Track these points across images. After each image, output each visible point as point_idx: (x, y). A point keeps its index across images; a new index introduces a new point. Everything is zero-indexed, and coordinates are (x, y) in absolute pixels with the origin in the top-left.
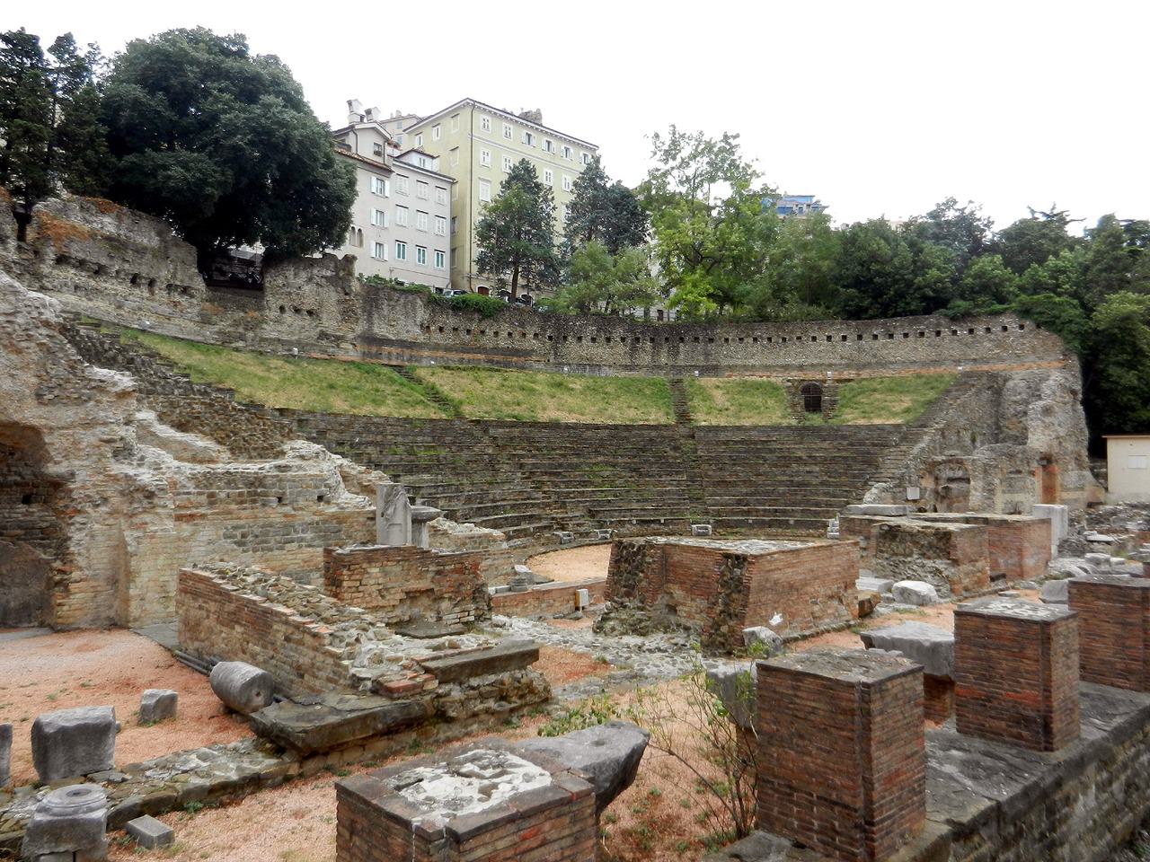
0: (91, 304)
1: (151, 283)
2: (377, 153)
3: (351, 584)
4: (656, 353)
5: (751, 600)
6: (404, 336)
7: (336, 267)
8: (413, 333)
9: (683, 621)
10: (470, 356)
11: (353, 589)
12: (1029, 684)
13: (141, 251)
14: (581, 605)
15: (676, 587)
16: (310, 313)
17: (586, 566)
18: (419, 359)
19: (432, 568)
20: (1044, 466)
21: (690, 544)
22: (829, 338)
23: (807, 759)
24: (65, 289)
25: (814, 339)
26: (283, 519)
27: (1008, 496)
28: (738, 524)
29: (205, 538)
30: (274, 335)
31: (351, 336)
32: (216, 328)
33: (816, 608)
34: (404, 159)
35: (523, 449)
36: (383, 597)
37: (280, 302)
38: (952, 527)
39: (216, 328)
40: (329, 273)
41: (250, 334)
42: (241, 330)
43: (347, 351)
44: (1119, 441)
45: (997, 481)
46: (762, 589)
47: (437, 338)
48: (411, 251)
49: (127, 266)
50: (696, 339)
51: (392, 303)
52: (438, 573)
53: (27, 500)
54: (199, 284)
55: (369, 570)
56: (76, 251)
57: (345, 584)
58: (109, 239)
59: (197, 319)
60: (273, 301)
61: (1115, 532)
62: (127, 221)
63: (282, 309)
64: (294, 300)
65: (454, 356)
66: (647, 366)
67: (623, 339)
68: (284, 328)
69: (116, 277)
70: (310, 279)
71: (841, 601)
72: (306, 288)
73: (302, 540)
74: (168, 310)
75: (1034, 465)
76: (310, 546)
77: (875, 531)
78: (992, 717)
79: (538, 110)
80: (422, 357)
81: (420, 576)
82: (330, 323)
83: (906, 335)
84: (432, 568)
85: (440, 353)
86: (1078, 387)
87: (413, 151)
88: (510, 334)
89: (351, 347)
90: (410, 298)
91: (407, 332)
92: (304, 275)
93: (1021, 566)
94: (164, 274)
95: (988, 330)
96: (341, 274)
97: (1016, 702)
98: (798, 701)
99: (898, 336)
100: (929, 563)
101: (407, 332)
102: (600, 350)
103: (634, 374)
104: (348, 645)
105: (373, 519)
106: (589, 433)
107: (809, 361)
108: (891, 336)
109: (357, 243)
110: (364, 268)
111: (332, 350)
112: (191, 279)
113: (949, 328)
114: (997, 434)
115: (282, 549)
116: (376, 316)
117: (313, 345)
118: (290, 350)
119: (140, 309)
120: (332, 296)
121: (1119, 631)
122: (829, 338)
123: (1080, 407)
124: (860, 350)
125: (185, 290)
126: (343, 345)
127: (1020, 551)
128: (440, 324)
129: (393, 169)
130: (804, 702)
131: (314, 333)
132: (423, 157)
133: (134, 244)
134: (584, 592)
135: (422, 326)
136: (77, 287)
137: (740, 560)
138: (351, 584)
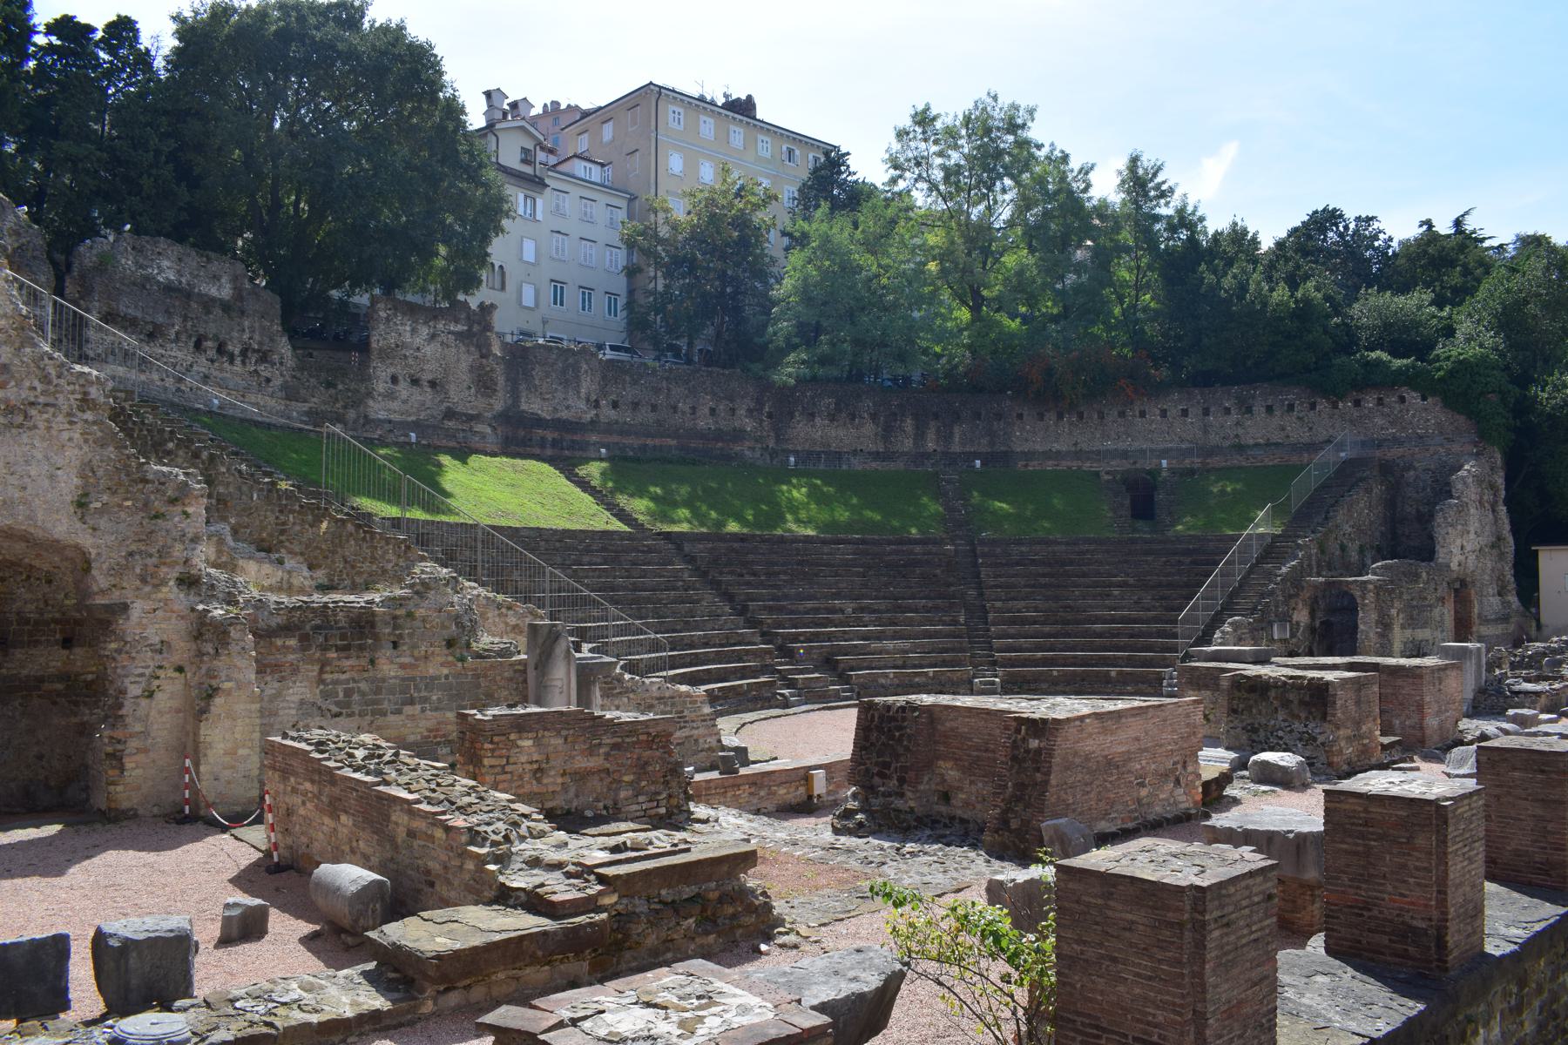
0: (143, 377)
2: (525, 161)
3: (493, 762)
4: (920, 435)
5: (1053, 782)
6: (564, 415)
7: (468, 318)
9: (959, 812)
10: (657, 442)
11: (498, 769)
12: (1418, 884)
13: (208, 303)
14: (816, 793)
15: (949, 764)
16: (433, 384)
17: (821, 737)
18: (584, 446)
19: (607, 740)
20: (1456, 590)
21: (969, 704)
22: (1164, 413)
23: (1121, 988)
24: (111, 358)
25: (1143, 414)
26: (401, 673)
27: (1408, 632)
28: (1037, 678)
29: (296, 698)
30: (382, 415)
31: (489, 415)
33: (1144, 792)
34: (560, 168)
35: (732, 573)
36: (539, 781)
37: (392, 370)
38: (1330, 676)
39: (305, 407)
40: (459, 328)
41: (351, 414)
44: (1554, 554)
45: (1394, 612)
46: (1068, 767)
47: (607, 413)
48: (572, 296)
50: (978, 416)
52: (615, 746)
53: (67, 643)
55: (520, 743)
56: (126, 307)
57: (486, 762)
58: (169, 288)
61: (1546, 679)
62: (193, 260)
63: (394, 380)
66: (904, 454)
67: (874, 417)
68: (395, 405)
69: (177, 340)
70: (433, 337)
71: (1177, 782)
72: (429, 350)
73: (425, 700)
75: (1443, 590)
76: (436, 709)
77: (1225, 684)
78: (1370, 930)
79: (749, 97)
80: (588, 443)
81: (591, 751)
82: (461, 395)
83: (1269, 409)
84: (607, 740)
85: (615, 438)
86: (1500, 481)
87: (575, 156)
88: (713, 411)
89: (489, 430)
91: (568, 407)
92: (424, 331)
93: (1422, 728)
95: (1380, 402)
96: (476, 328)
97: (1401, 909)
98: (1110, 913)
99: (1260, 410)
100: (1298, 726)
101: (568, 407)
102: (841, 433)
103: (892, 466)
104: (495, 844)
105: (525, 671)
107: (1136, 445)
108: (1249, 410)
109: (497, 284)
110: (506, 323)
112: (272, 340)
113: (1328, 399)
114: (1391, 546)
115: (399, 712)
116: (523, 387)
117: (434, 427)
118: (407, 435)
120: (463, 360)
121: (1539, 812)
122: (1164, 413)
123: (1502, 509)
124: (1206, 432)
126: (479, 428)
127: (1420, 707)
128: (613, 397)
129: (547, 181)
130: (1118, 915)
132: (589, 165)
133: (200, 295)
134: (820, 774)
135: (588, 400)
137: (1040, 727)
138: (493, 762)
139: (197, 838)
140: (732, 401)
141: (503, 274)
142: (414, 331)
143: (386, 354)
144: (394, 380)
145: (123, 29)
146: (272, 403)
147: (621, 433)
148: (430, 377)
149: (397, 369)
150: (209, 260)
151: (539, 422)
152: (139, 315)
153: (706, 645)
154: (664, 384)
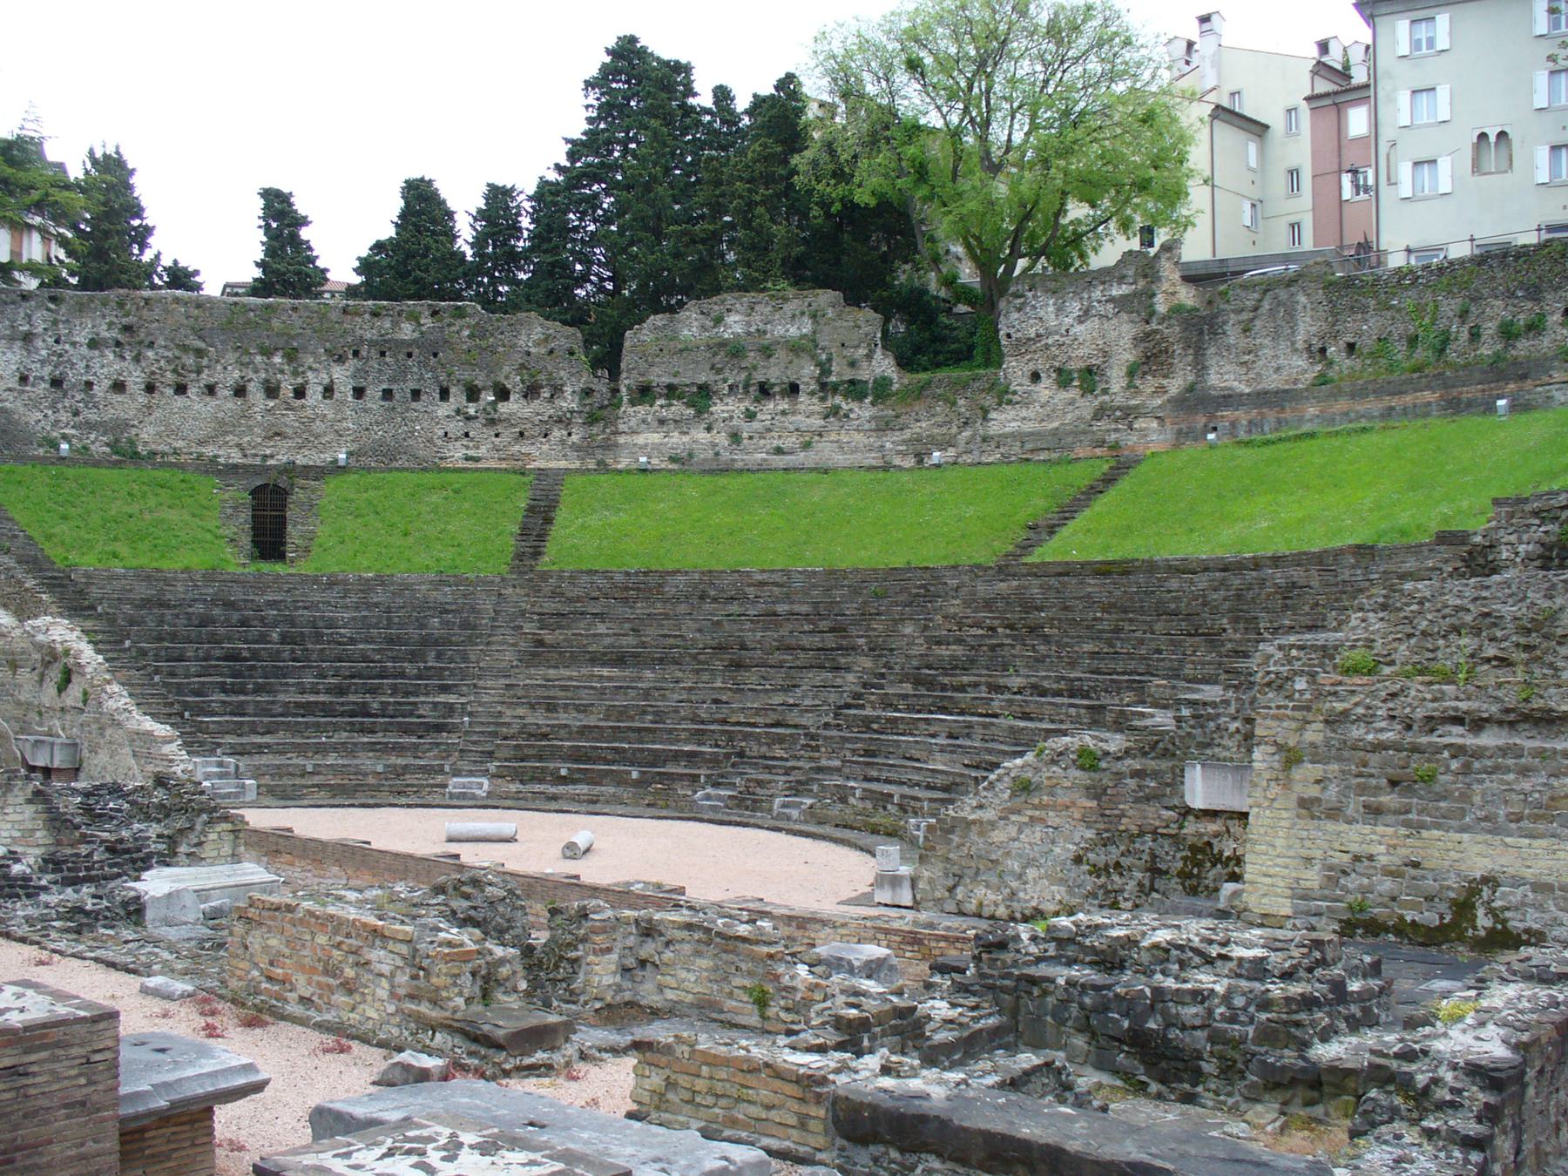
0: (686, 439)
1: (793, 389)
6: (1272, 382)
8: (1298, 368)
27: (1379, 841)
32: (907, 434)
37: (1031, 366)
39: (907, 434)
40: (1125, 289)
41: (966, 434)
42: (954, 430)
43: (1144, 433)
51: (1245, 316)
56: (659, 376)
59: (867, 426)
60: (1015, 370)
64: (1054, 358)
65: (1373, 405)
72: (1078, 329)
74: (817, 422)
89: (1155, 424)
90: (1283, 294)
106: (1174, 584)
111: (1114, 436)
112: (852, 364)
119: (769, 430)
131: (1087, 414)
135: (1309, 349)
136: (662, 422)
139: (617, 884)
140: (1537, 300)
141: (1509, 142)
142: (1060, 310)
143: (1023, 346)
144: (1035, 377)
145: (788, 83)
146: (859, 438)
147: (1353, 396)
148: (1081, 365)
151: (1230, 399)
152: (675, 381)
153: (724, 722)
154: (1429, 296)
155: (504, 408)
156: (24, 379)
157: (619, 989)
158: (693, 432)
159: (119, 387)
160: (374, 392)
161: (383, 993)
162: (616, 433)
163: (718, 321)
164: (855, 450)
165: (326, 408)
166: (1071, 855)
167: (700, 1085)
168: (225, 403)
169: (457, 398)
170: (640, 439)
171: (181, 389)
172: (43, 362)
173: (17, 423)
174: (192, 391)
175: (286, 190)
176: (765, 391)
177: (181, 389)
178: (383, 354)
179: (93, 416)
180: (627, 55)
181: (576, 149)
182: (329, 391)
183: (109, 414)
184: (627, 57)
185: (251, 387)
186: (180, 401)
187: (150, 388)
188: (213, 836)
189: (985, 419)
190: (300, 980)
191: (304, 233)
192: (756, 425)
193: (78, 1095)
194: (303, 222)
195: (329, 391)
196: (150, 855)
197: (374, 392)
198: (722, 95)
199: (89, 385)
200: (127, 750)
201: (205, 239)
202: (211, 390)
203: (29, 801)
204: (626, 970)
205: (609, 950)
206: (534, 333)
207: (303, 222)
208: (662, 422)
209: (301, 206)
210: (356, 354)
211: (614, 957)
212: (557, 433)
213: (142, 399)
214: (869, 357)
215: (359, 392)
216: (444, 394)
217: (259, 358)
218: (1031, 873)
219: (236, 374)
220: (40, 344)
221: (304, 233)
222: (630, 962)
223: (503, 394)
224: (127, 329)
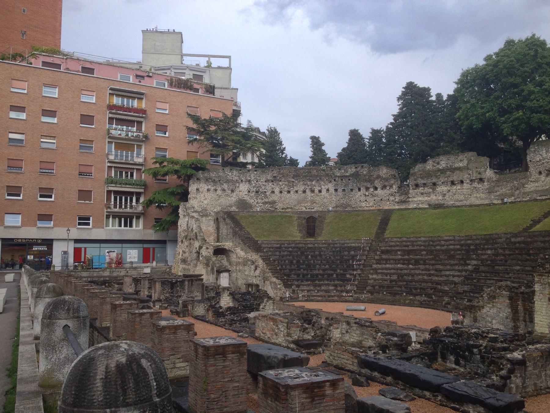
0: (429, 198)
1: (462, 182)
13: (453, 170)
32: (498, 193)
39: (498, 193)
41: (518, 192)
49: (446, 179)
54: (489, 173)
56: (420, 181)
94: (465, 176)
112: (480, 173)
125: (481, 180)
136: (422, 194)
144: (540, 173)
149: (541, 169)
150: (458, 156)
152: (425, 182)
155: (376, 192)
156: (249, 192)
157: (341, 338)
158: (431, 197)
159: (273, 192)
160: (340, 190)
161: (282, 335)
162: (409, 198)
163: (438, 163)
164: (483, 199)
165: (327, 195)
166: (504, 316)
167: (335, 355)
168: (301, 195)
169: (363, 190)
170: (415, 199)
171: (289, 192)
172: (254, 187)
173: (248, 203)
174: (292, 192)
175: (317, 136)
176: (453, 183)
177: (289, 192)
178: (342, 180)
179: (267, 200)
180: (411, 88)
181: (396, 117)
182: (328, 190)
183: (271, 199)
184: (411, 88)
185: (307, 191)
186: (289, 195)
187: (281, 192)
188: (268, 304)
189: (523, 187)
190: (268, 333)
191: (323, 148)
192: (450, 193)
193: (186, 339)
194: (323, 144)
195: (328, 190)
196: (254, 308)
197: (340, 190)
198: (439, 96)
199: (265, 192)
200: (270, 287)
201: (297, 150)
202: (297, 192)
203: (228, 296)
204: (343, 334)
205: (338, 328)
206: (384, 171)
207: (323, 144)
208: (422, 194)
209: (322, 140)
210: (335, 180)
211: (339, 330)
212: (392, 198)
213: (279, 195)
214: (485, 171)
215: (336, 190)
216: (359, 190)
217: (309, 183)
218: (494, 321)
219: (303, 187)
220: (253, 182)
221: (323, 148)
222: (344, 332)
223: (376, 189)
224: (275, 177)
